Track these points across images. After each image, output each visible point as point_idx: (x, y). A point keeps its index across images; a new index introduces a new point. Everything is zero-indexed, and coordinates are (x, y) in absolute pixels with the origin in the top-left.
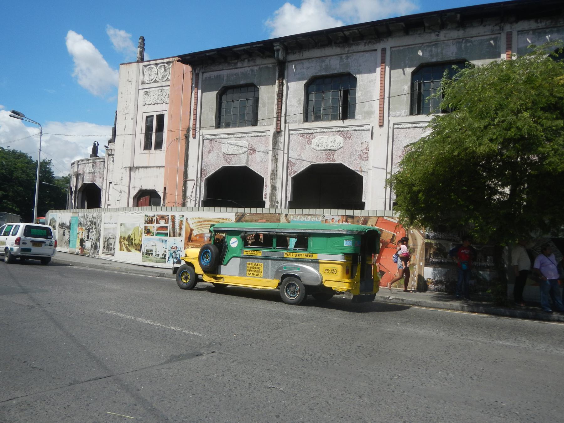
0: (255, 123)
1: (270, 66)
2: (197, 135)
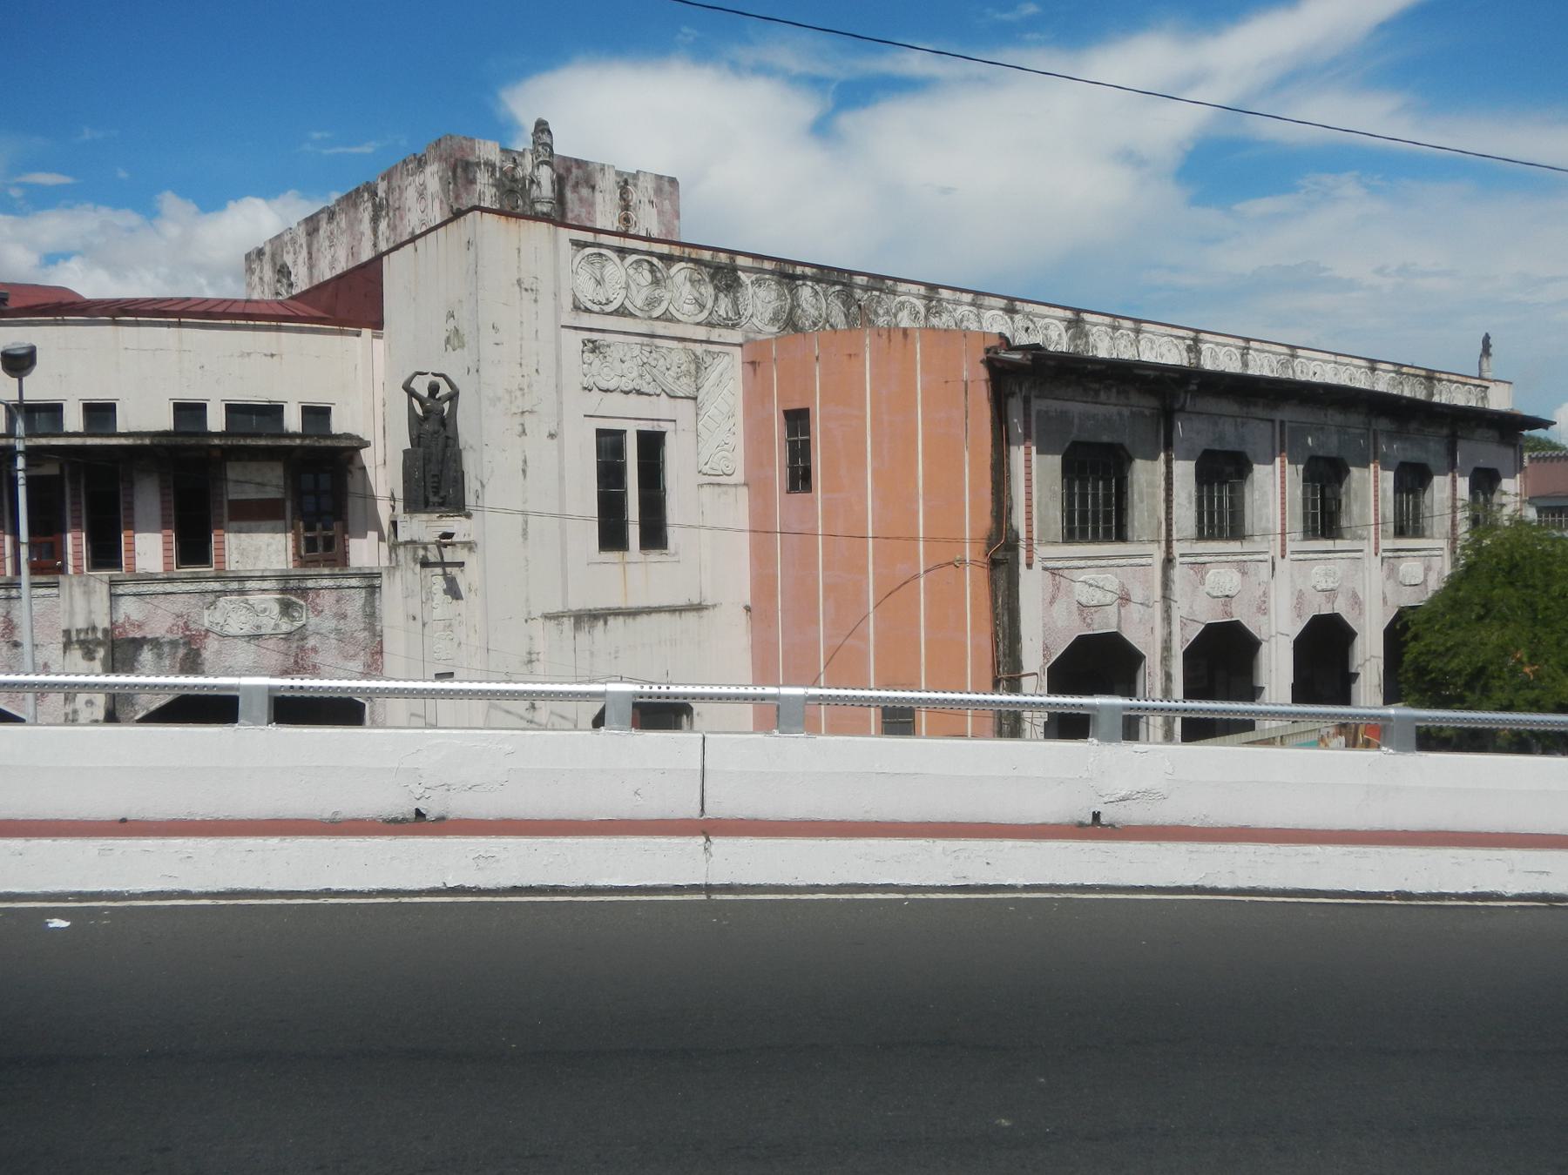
0: (1121, 537)
1: (1147, 412)
2: (1036, 558)
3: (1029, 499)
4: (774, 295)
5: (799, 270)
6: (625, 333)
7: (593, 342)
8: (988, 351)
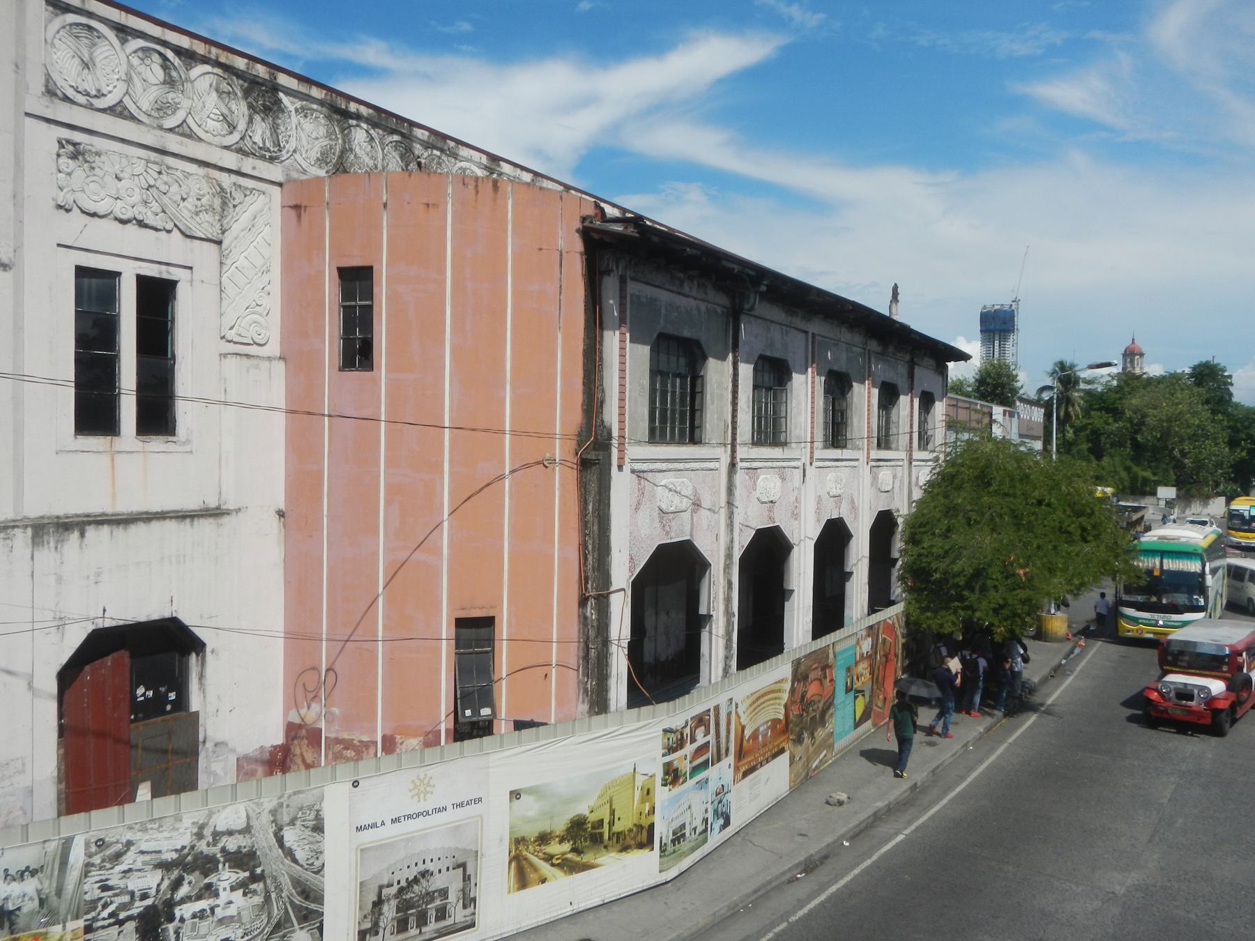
3: (622, 393)
4: (322, 131)
5: (353, 107)
6: (123, 141)
7: (75, 144)
8: (584, 219)
